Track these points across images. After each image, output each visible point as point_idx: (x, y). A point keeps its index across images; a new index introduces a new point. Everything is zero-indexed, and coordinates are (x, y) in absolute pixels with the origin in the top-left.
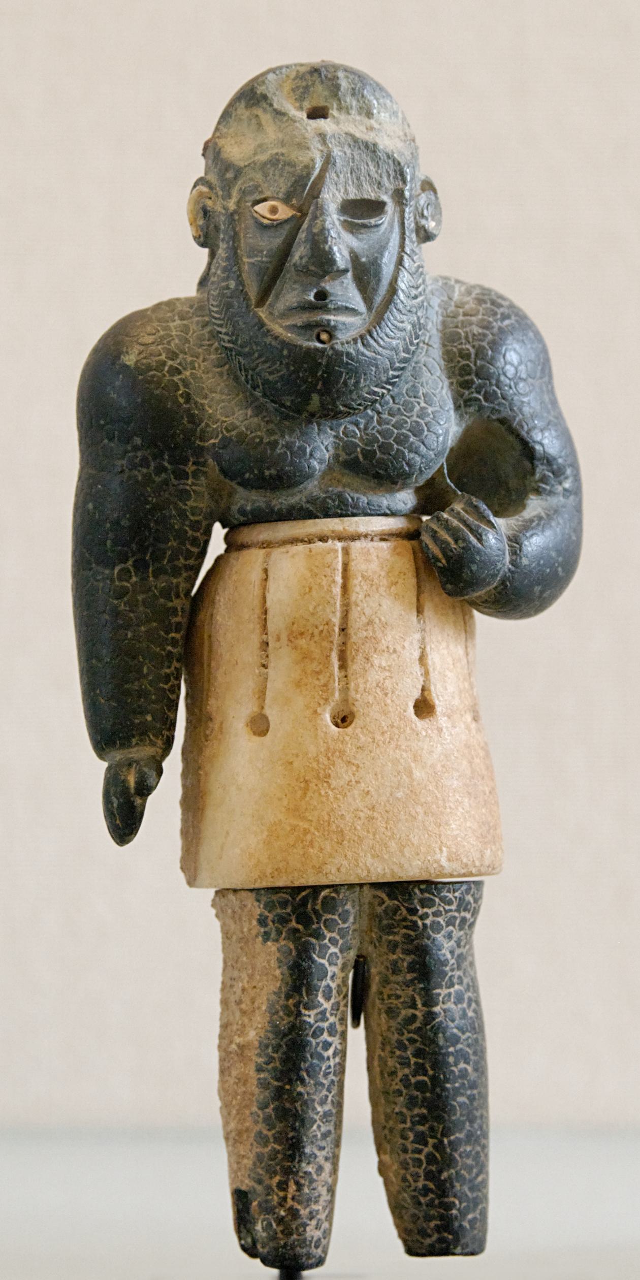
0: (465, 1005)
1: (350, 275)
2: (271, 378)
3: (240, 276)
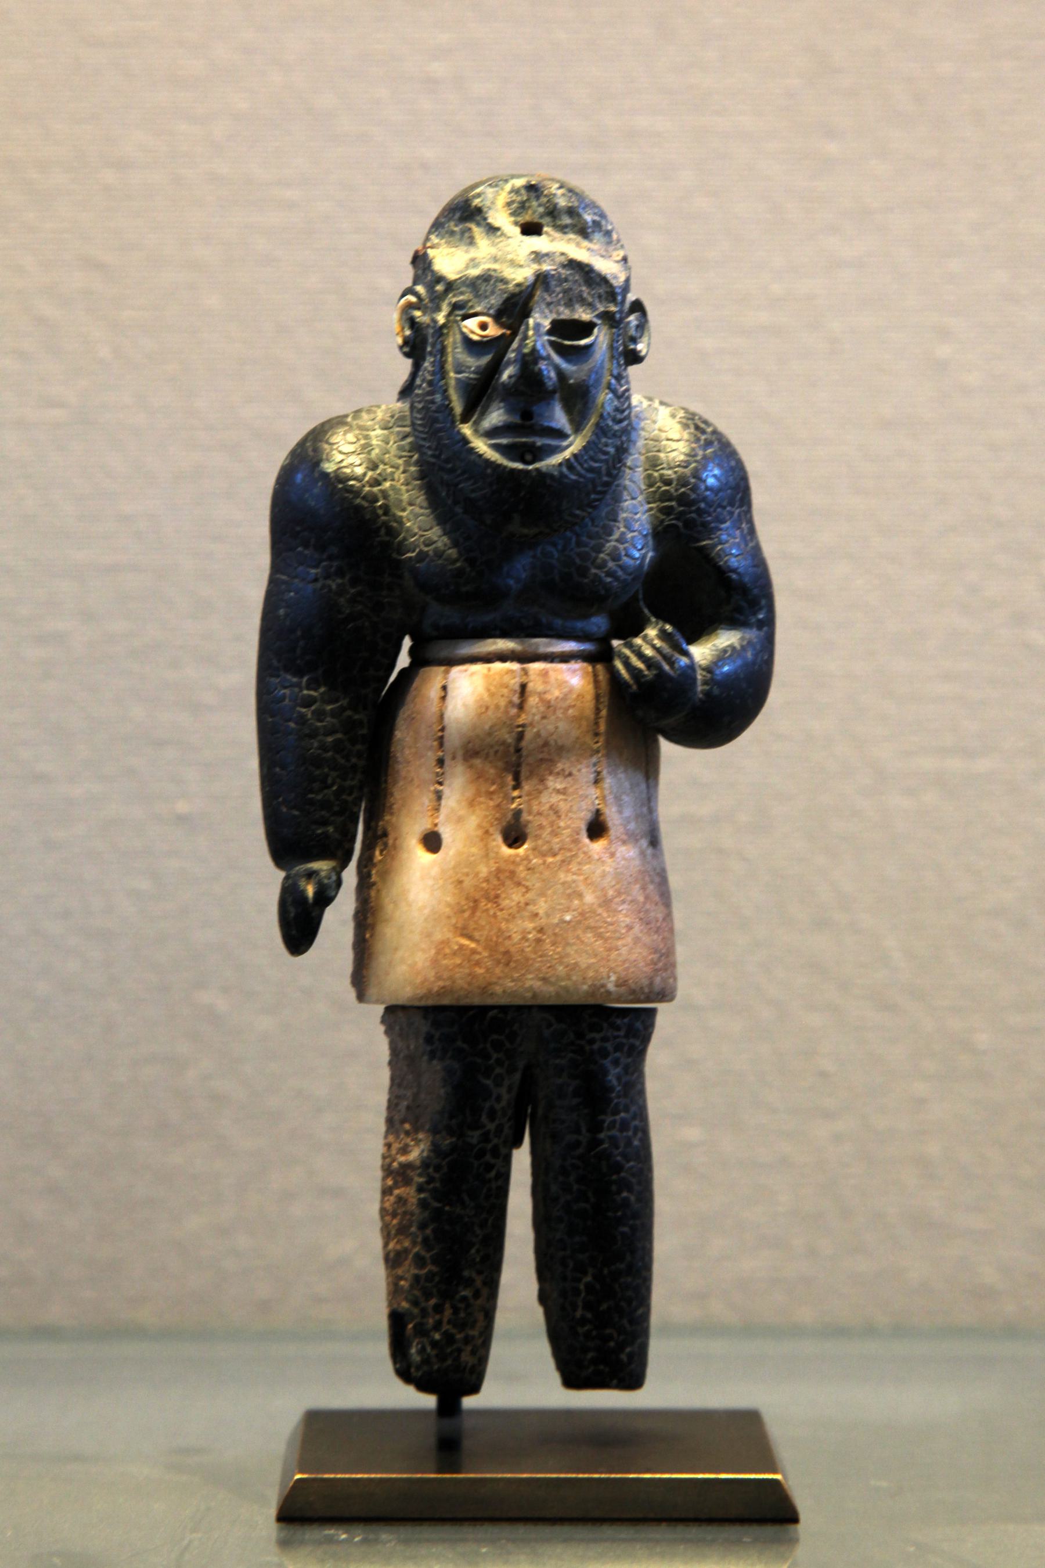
0: (630, 1133)
1: (557, 396)
2: (473, 495)
3: (446, 391)
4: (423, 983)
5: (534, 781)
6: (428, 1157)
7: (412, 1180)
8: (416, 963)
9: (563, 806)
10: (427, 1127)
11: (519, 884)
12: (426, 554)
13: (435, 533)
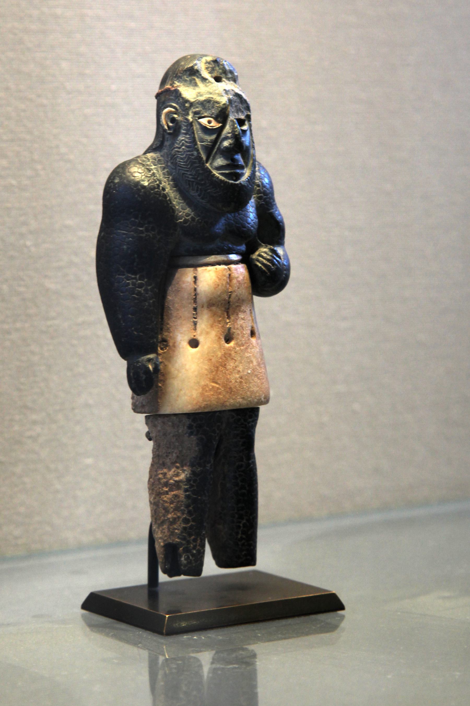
2: (214, 195)
4: (196, 404)
5: (235, 315)
6: (190, 477)
7: (181, 487)
8: (192, 395)
9: (244, 325)
10: (188, 464)
11: (233, 359)
12: (188, 220)
13: (188, 210)
